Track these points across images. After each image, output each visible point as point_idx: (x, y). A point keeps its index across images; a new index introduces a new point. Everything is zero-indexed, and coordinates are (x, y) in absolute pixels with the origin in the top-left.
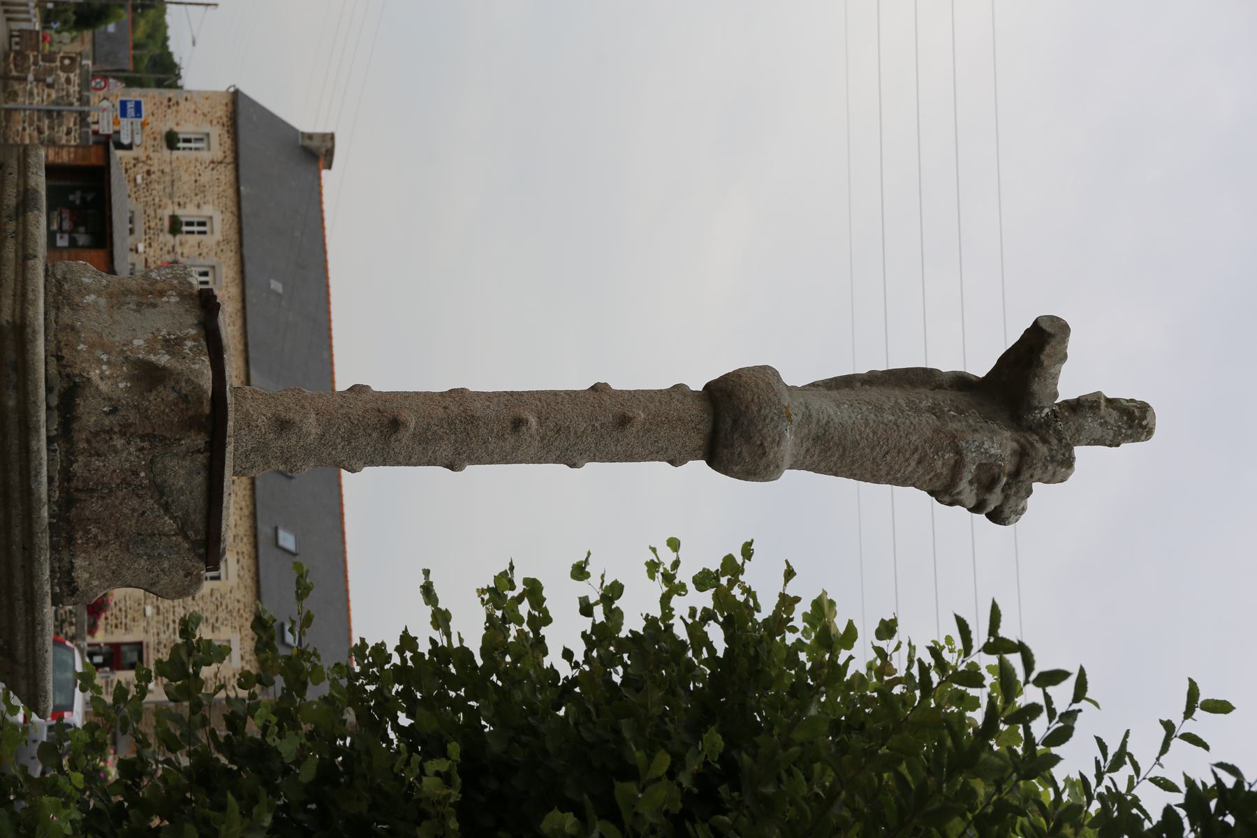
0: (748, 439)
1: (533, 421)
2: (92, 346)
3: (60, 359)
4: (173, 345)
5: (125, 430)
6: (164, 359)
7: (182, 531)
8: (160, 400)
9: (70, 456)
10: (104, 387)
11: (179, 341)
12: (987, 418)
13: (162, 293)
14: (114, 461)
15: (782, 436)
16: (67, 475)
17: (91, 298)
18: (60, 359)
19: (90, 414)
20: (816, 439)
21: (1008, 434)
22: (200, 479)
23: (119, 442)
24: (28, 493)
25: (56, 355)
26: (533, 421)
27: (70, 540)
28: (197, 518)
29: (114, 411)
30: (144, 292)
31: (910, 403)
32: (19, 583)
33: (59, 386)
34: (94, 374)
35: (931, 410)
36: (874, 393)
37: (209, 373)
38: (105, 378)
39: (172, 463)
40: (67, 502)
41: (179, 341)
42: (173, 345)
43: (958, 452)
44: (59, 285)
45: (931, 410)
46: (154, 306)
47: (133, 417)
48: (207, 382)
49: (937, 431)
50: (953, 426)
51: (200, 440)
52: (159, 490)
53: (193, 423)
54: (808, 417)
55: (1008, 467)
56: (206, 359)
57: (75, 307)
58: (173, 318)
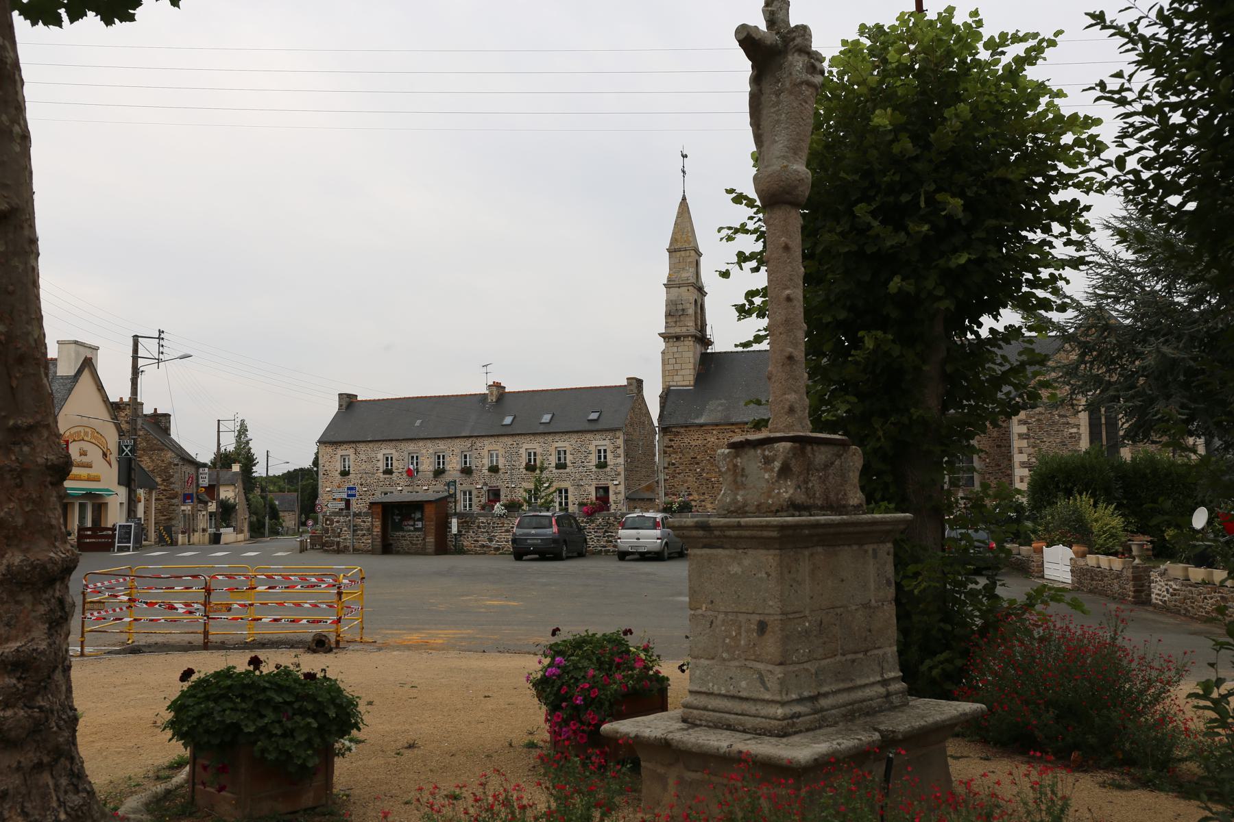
0: (796, 187)
1: (788, 292)
2: (769, 497)
3: (778, 511)
4: (768, 461)
5: (806, 482)
6: (777, 465)
7: (840, 456)
8: (795, 466)
9: (816, 507)
10: (791, 491)
11: (765, 457)
12: (780, 67)
13: (735, 466)
14: (817, 487)
15: (795, 170)
16: (822, 508)
17: (739, 498)
18: (778, 511)
19: (801, 498)
20: (795, 153)
21: (790, 58)
22: (823, 449)
23: (810, 485)
24: (839, 524)
25: (776, 513)
26: (788, 292)
27: (844, 506)
28: (836, 449)
29: (799, 487)
30: (735, 474)
31: (773, 106)
32: (866, 529)
33: (792, 511)
34: (786, 496)
35: (778, 95)
36: (766, 124)
37: (783, 444)
38: (787, 491)
39: (817, 461)
40: (830, 507)
41: (765, 457)
42: (768, 461)
43: (802, 83)
44: (732, 512)
45: (778, 95)
46: (743, 469)
47: (801, 478)
48: (789, 444)
49: (791, 93)
50: (788, 85)
51: (809, 448)
52: (827, 466)
53: (803, 450)
54: (784, 157)
55: (806, 58)
56: (776, 445)
57: (745, 505)
58: (751, 461)
